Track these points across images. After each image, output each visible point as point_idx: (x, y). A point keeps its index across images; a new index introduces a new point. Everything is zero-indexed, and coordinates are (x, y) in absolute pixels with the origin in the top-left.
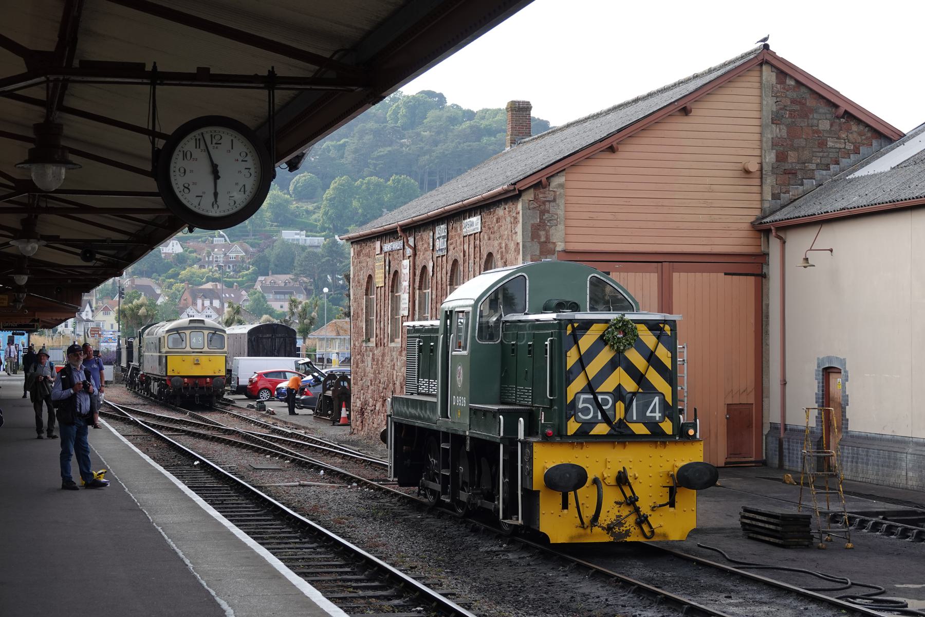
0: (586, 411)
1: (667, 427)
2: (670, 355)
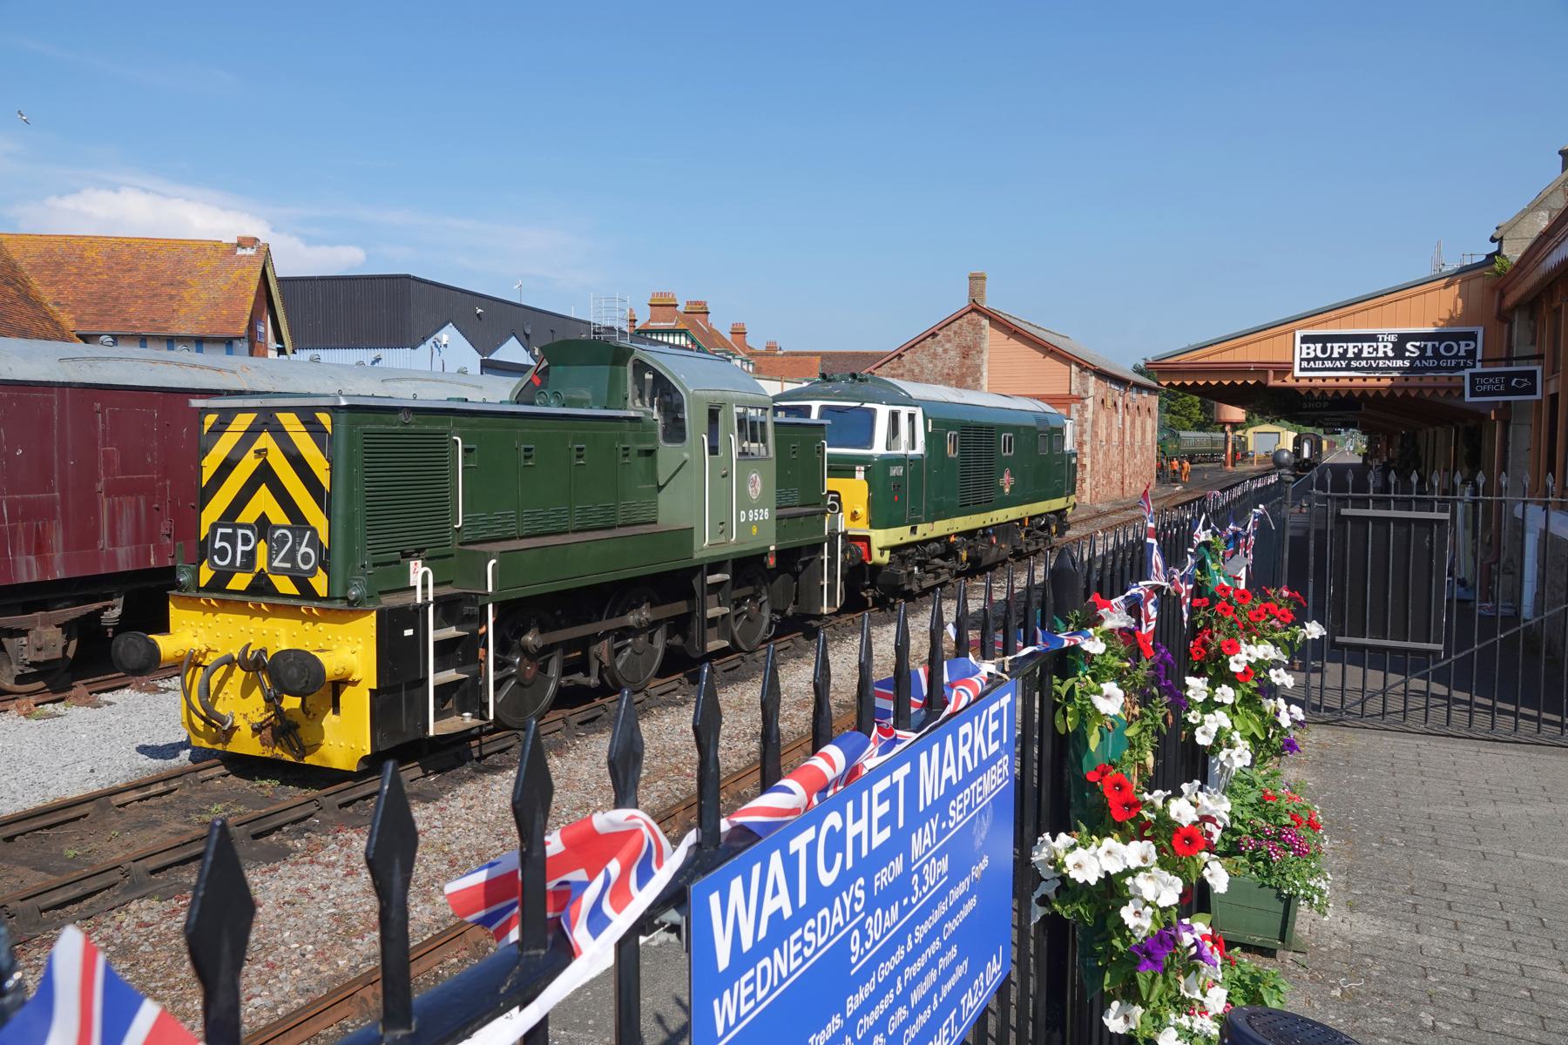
0: (222, 553)
1: (320, 583)
2: (327, 465)
